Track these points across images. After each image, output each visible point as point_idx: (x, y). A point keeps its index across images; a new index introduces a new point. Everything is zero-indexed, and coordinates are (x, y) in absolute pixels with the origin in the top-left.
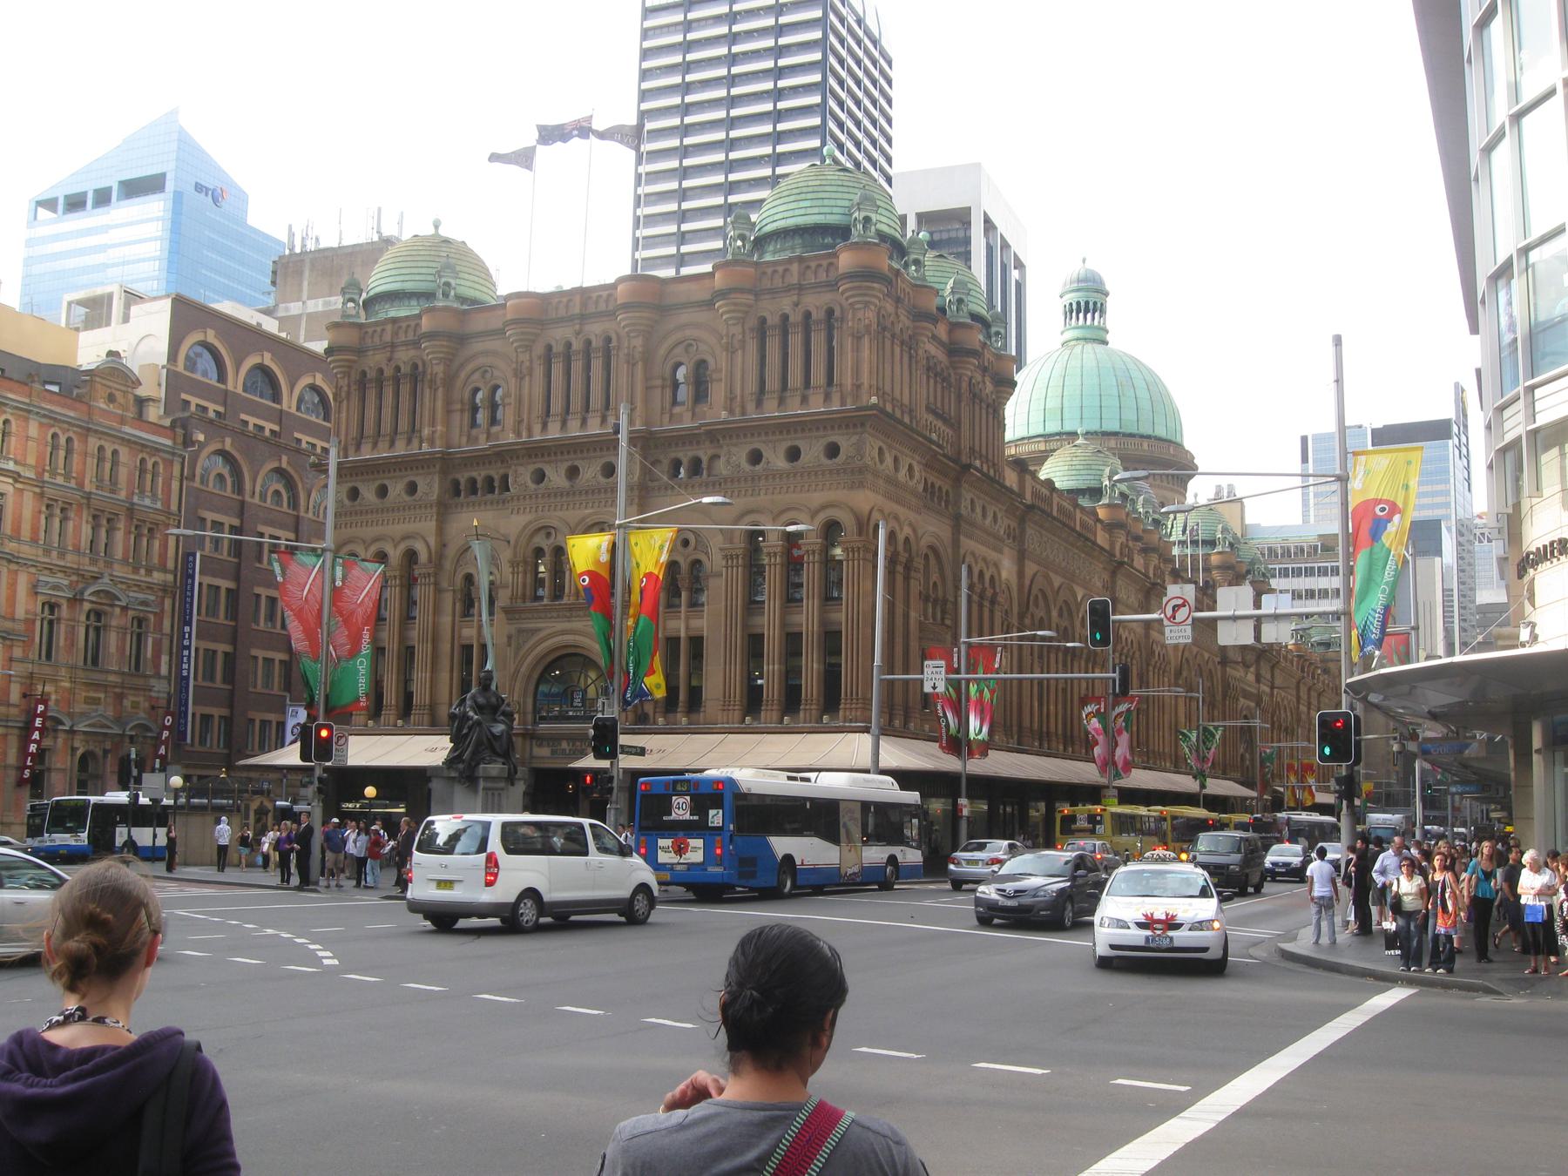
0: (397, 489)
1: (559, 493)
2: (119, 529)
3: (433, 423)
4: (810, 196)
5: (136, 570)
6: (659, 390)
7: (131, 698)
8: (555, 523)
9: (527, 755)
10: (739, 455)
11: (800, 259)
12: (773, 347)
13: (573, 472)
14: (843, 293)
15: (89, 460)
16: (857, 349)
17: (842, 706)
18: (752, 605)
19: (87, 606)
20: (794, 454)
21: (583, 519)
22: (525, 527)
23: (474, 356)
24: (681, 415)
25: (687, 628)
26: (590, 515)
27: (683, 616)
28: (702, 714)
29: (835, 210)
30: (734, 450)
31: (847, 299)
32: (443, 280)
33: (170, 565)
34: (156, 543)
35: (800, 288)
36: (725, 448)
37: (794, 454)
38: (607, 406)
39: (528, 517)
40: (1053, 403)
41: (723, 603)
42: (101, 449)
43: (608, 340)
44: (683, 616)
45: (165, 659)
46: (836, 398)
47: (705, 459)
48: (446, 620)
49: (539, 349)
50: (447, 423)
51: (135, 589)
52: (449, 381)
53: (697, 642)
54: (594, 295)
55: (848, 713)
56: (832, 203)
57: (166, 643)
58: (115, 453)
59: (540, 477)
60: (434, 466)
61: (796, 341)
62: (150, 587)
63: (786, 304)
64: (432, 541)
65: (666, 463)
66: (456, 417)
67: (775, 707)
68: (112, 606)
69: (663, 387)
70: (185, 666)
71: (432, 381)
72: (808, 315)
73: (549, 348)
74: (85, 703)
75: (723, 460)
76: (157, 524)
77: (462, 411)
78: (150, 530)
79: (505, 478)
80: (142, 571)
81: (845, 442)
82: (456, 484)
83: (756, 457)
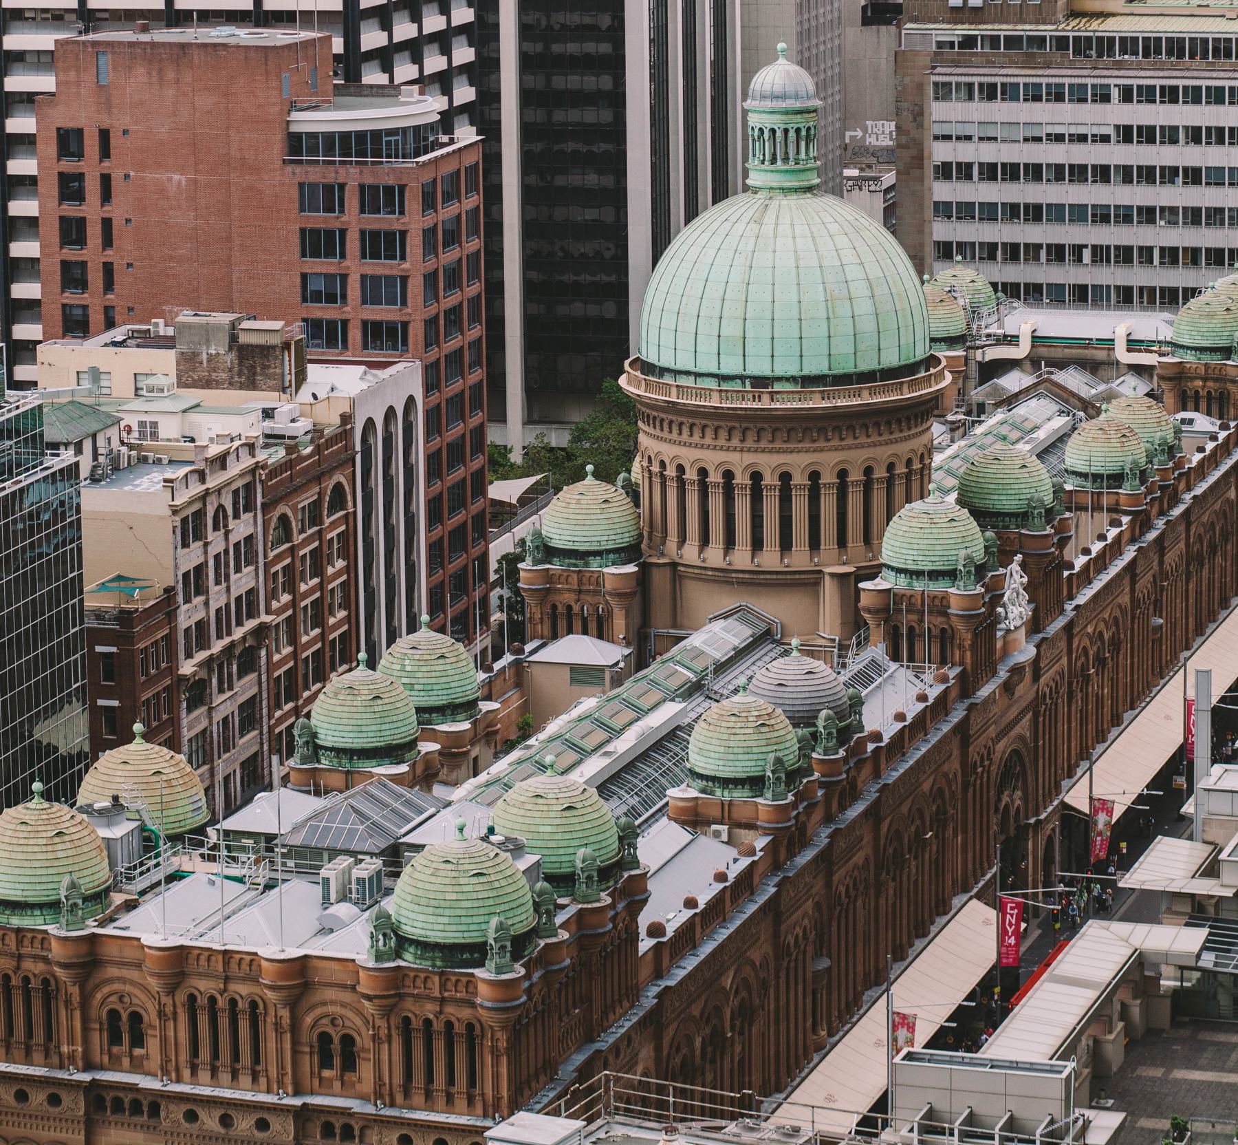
3: (71, 1042)
4: (447, 912)
16: (496, 1064)
23: (110, 981)
24: (330, 1080)
29: (472, 927)
38: (256, 1060)
40: (731, 329)
43: (254, 1005)
50: (86, 1042)
52: (85, 1005)
54: (238, 956)
56: (469, 920)
61: (439, 1046)
63: (429, 1010)
66: (95, 1038)
71: (68, 1003)
72: (449, 1025)
73: (192, 998)
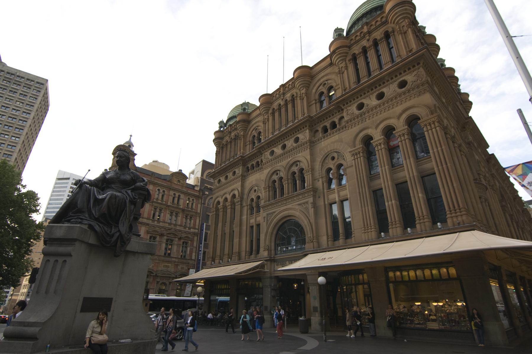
0: (230, 175)
1: (280, 156)
2: (180, 216)
5: (185, 227)
6: (314, 104)
7: (181, 266)
8: (278, 168)
9: (273, 270)
10: (353, 109)
11: (367, 24)
13: (284, 147)
14: (391, 23)
15: (170, 197)
17: (448, 216)
18: (372, 177)
19: (165, 237)
20: (381, 96)
21: (289, 162)
22: (268, 173)
25: (339, 196)
26: (291, 160)
28: (353, 238)
30: (349, 108)
31: (394, 23)
32: (243, 107)
33: (197, 227)
34: (192, 221)
35: (369, 33)
36: (345, 110)
37: (381, 96)
39: (269, 169)
41: (356, 177)
42: (174, 194)
45: (194, 254)
48: (244, 217)
51: (184, 233)
55: (455, 219)
57: (194, 249)
58: (179, 196)
59: (272, 153)
60: (240, 164)
62: (189, 233)
64: (240, 189)
65: (320, 129)
67: (398, 225)
68: (175, 238)
69: (316, 103)
70: (200, 256)
74: (163, 267)
76: (193, 216)
77: (250, 144)
78: (191, 218)
80: (187, 229)
81: (409, 78)
82: (248, 167)
83: (361, 106)
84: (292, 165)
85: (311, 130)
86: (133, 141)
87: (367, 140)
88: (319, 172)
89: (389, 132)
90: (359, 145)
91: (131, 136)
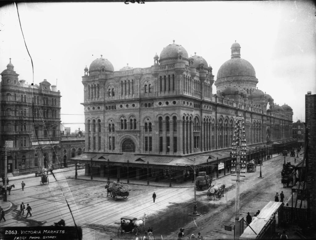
12: (163, 82)
27: (148, 133)
30: (156, 102)
44: (148, 133)
46: (175, 92)
47: (151, 103)
49: (120, 82)
53: (151, 138)
59: (121, 106)
75: (154, 104)
77: (107, 93)
79: (115, 106)
81: (177, 101)
83: (160, 104)
84: (131, 116)
85: (140, 104)
86: (13, 63)
87: (160, 118)
88: (143, 124)
89: (167, 118)
90: (157, 120)
91: (10, 59)
